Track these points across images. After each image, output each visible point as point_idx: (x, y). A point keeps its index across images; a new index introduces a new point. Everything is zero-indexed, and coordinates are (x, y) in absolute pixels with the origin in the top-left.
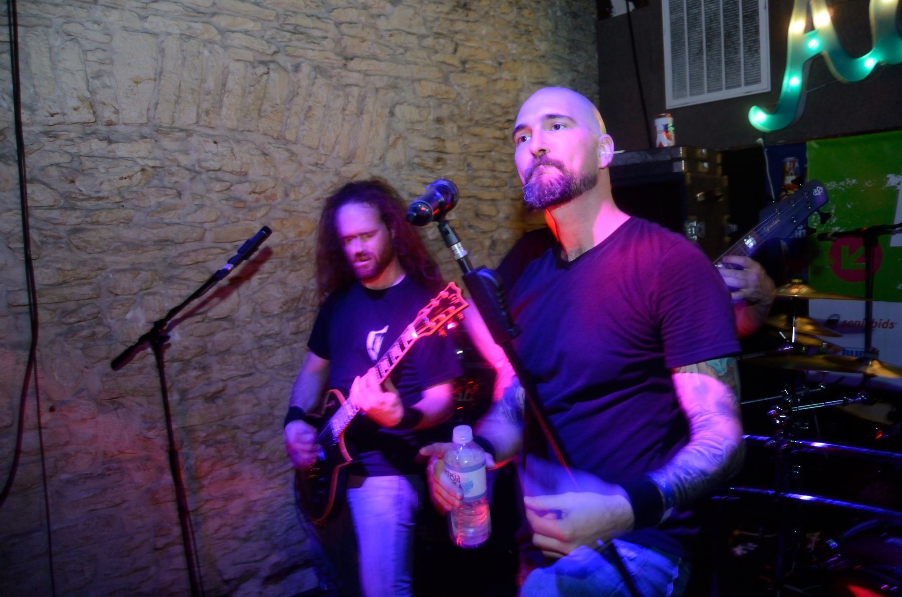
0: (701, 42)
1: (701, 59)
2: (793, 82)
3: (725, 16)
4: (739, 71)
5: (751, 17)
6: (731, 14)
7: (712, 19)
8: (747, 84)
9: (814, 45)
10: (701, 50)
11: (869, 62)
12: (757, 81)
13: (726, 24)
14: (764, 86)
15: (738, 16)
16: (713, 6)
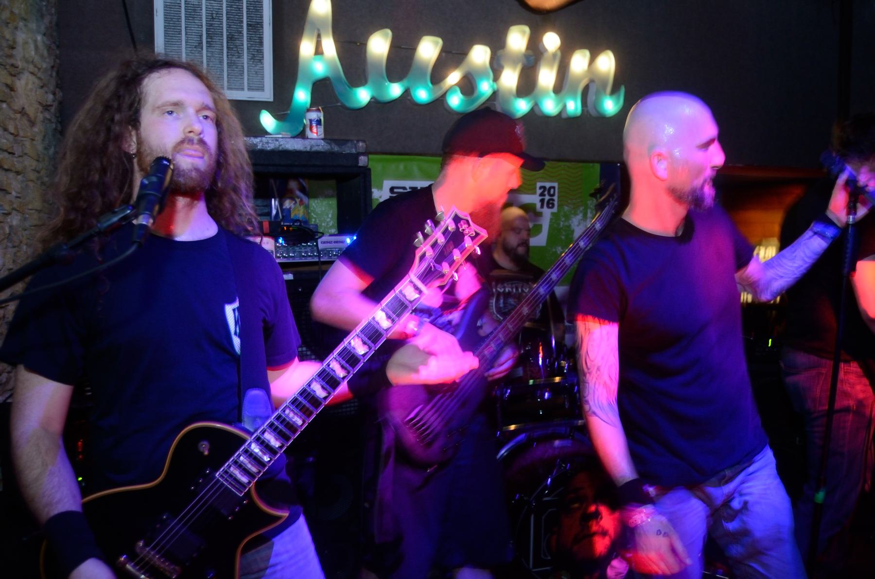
0: (201, 36)
1: (201, 53)
2: (302, 96)
3: (228, 18)
4: (242, 74)
5: (256, 27)
6: (234, 17)
7: (214, 17)
8: (250, 89)
9: (319, 69)
10: (201, 43)
11: (363, 96)
12: (261, 88)
13: (229, 26)
14: (267, 94)
15: (242, 22)
16: (215, 4)
